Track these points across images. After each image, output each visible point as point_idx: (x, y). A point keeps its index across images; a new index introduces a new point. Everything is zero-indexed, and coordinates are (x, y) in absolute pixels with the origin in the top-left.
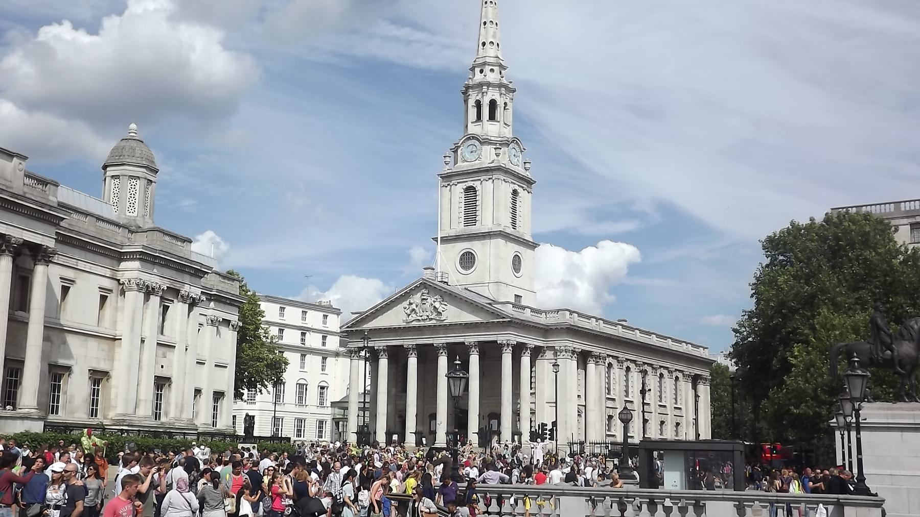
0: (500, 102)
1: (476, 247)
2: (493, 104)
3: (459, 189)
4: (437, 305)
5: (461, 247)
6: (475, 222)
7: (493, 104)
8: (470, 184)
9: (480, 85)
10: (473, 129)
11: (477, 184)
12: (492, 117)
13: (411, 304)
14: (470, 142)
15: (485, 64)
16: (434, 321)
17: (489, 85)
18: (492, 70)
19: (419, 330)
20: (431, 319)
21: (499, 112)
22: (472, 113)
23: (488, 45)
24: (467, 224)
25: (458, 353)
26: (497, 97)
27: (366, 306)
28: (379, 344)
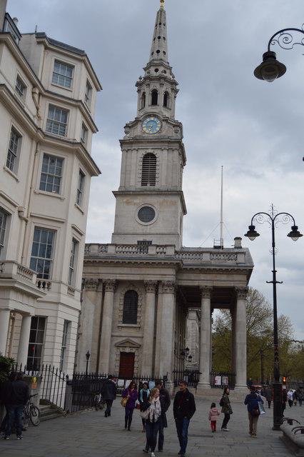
0: (172, 94)
3: (137, 157)
5: (140, 202)
6: (153, 184)
7: (166, 95)
8: (150, 151)
9: (159, 78)
10: (149, 109)
11: (158, 153)
12: (165, 105)
14: (152, 119)
17: (165, 79)
18: (165, 72)
21: (169, 103)
22: (149, 99)
23: (161, 53)
24: (144, 184)
26: (169, 91)
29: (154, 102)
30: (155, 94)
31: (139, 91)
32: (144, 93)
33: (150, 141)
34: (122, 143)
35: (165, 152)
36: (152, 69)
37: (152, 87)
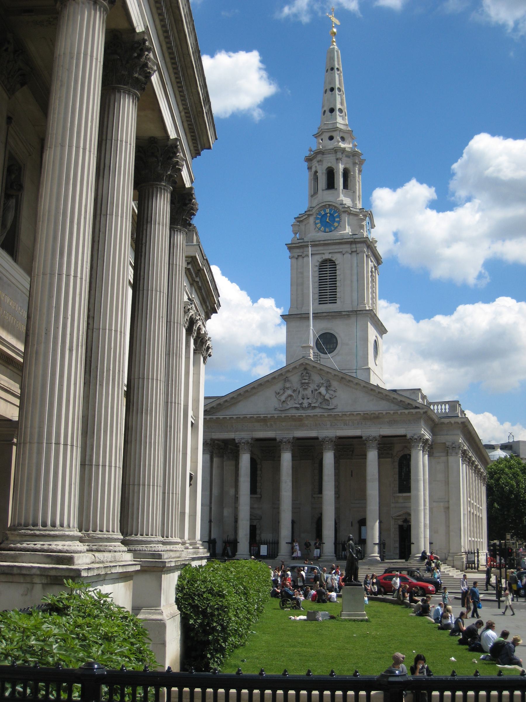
1: (338, 328)
2: (346, 173)
3: (311, 265)
4: (323, 390)
7: (346, 173)
8: (327, 256)
13: (288, 388)
15: (336, 129)
16: (317, 410)
18: (343, 139)
19: (300, 419)
20: (315, 407)
25: (349, 450)
26: (350, 166)
27: (223, 391)
28: (240, 435)
29: (331, 185)
30: (331, 174)
31: (310, 168)
32: (316, 172)
33: (326, 244)
34: (291, 247)
35: (348, 256)
36: (326, 135)
37: (326, 165)
